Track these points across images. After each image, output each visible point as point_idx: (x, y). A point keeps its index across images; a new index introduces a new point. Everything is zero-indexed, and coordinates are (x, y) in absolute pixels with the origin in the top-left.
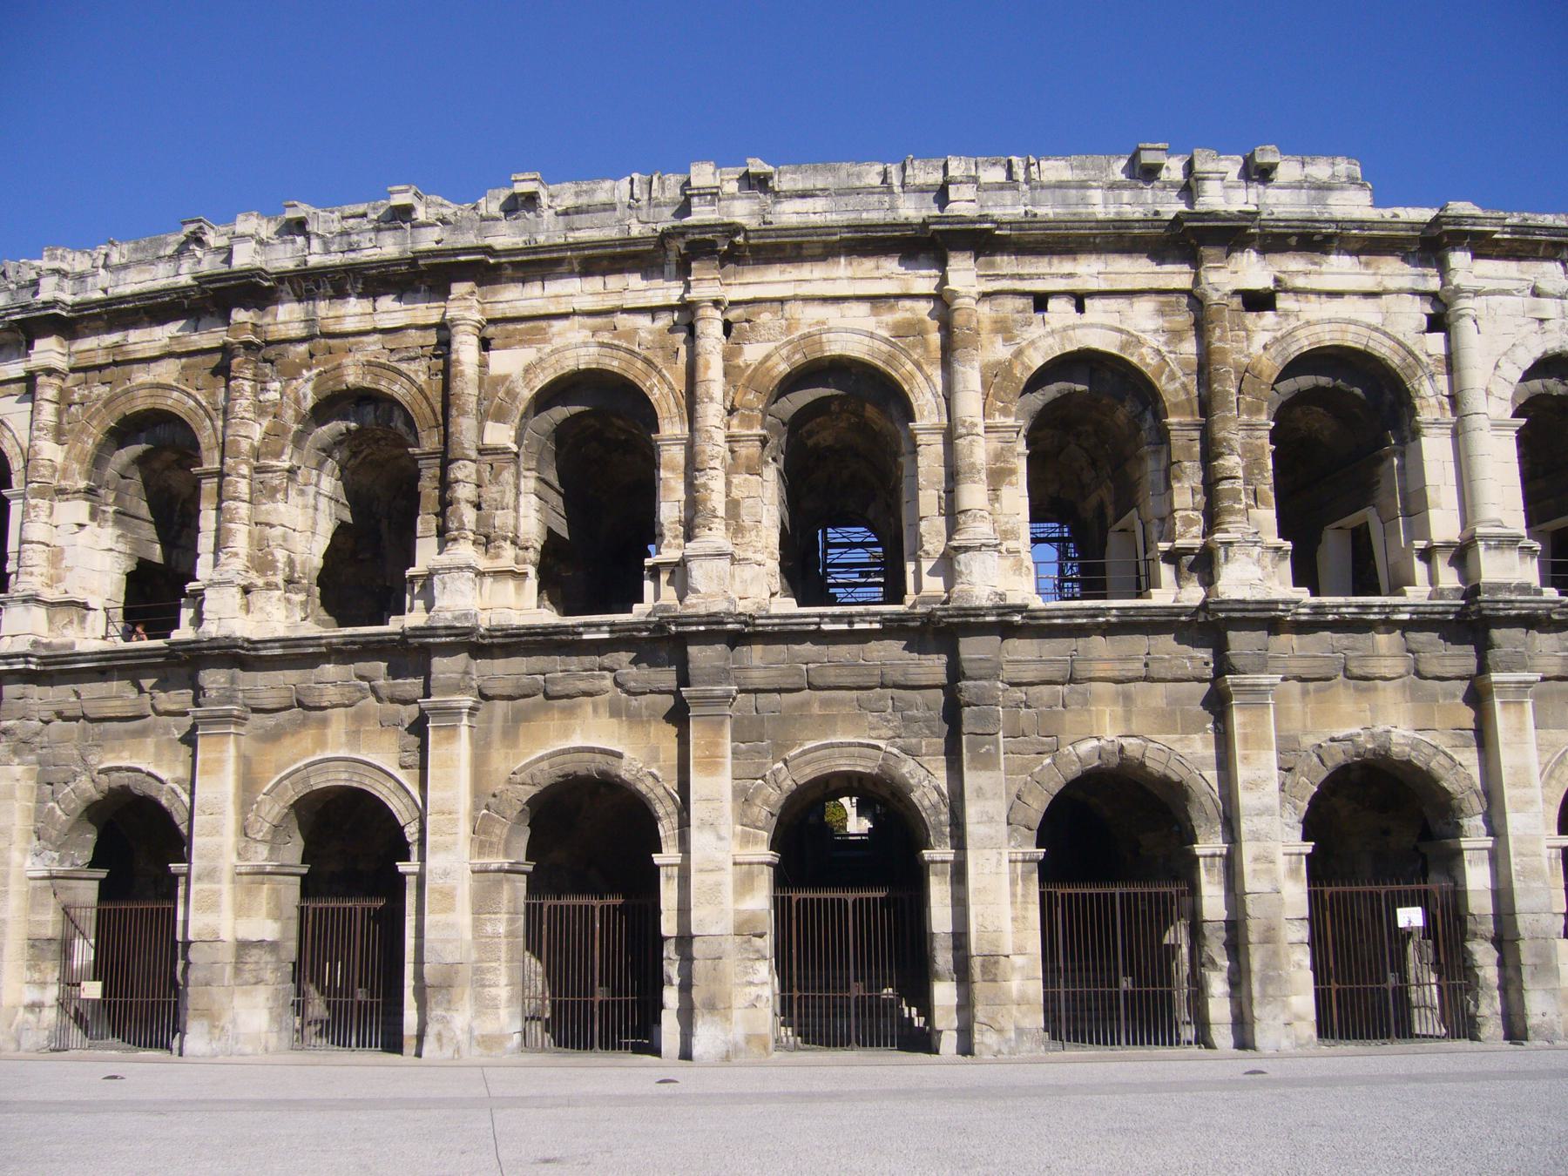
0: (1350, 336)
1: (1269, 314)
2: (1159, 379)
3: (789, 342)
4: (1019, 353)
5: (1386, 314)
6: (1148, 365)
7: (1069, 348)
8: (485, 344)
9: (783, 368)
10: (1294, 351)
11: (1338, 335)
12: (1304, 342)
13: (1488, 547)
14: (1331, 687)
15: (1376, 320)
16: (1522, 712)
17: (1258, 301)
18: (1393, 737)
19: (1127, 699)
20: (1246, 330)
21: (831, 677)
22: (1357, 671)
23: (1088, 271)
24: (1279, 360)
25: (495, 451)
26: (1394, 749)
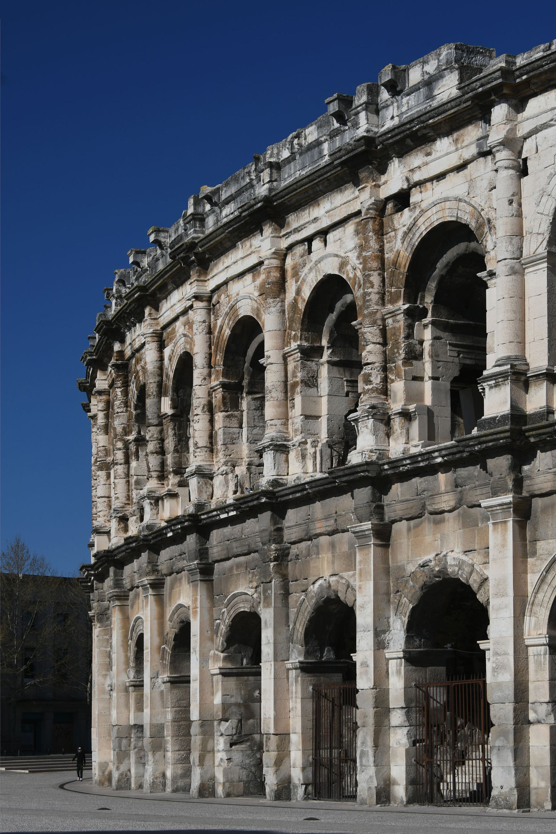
0: (447, 212)
2: (354, 289)
3: (227, 314)
6: (350, 279)
7: (320, 278)
9: (227, 332)
11: (440, 215)
13: (491, 387)
14: (421, 523)
16: (505, 530)
18: (450, 561)
19: (333, 546)
20: (395, 230)
21: (236, 548)
22: (430, 508)
24: (409, 250)
25: (165, 416)
26: (450, 570)
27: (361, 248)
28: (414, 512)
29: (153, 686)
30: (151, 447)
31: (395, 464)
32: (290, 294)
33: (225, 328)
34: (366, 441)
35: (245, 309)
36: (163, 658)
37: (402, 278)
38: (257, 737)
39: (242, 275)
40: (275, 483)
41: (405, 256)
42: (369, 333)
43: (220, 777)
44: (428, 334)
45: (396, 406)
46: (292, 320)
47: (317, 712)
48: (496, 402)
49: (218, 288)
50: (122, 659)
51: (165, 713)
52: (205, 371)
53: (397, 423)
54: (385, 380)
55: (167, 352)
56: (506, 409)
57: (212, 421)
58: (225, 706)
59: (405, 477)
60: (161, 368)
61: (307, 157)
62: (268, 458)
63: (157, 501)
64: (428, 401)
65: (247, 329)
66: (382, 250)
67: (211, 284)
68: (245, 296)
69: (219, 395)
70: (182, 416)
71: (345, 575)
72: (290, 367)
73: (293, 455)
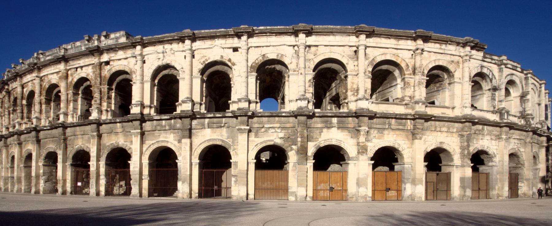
1: (109, 66)
4: (73, 79)
5: (129, 63)
9: (47, 86)
10: (112, 72)
12: (114, 70)
15: (126, 64)
17: (107, 63)
23: (82, 62)
27: (94, 72)
30: (18, 111)
32: (70, 79)
33: (46, 85)
35: (54, 81)
57: (41, 107)
63: (20, 124)
65: (54, 86)
66: (100, 74)
70: (30, 105)
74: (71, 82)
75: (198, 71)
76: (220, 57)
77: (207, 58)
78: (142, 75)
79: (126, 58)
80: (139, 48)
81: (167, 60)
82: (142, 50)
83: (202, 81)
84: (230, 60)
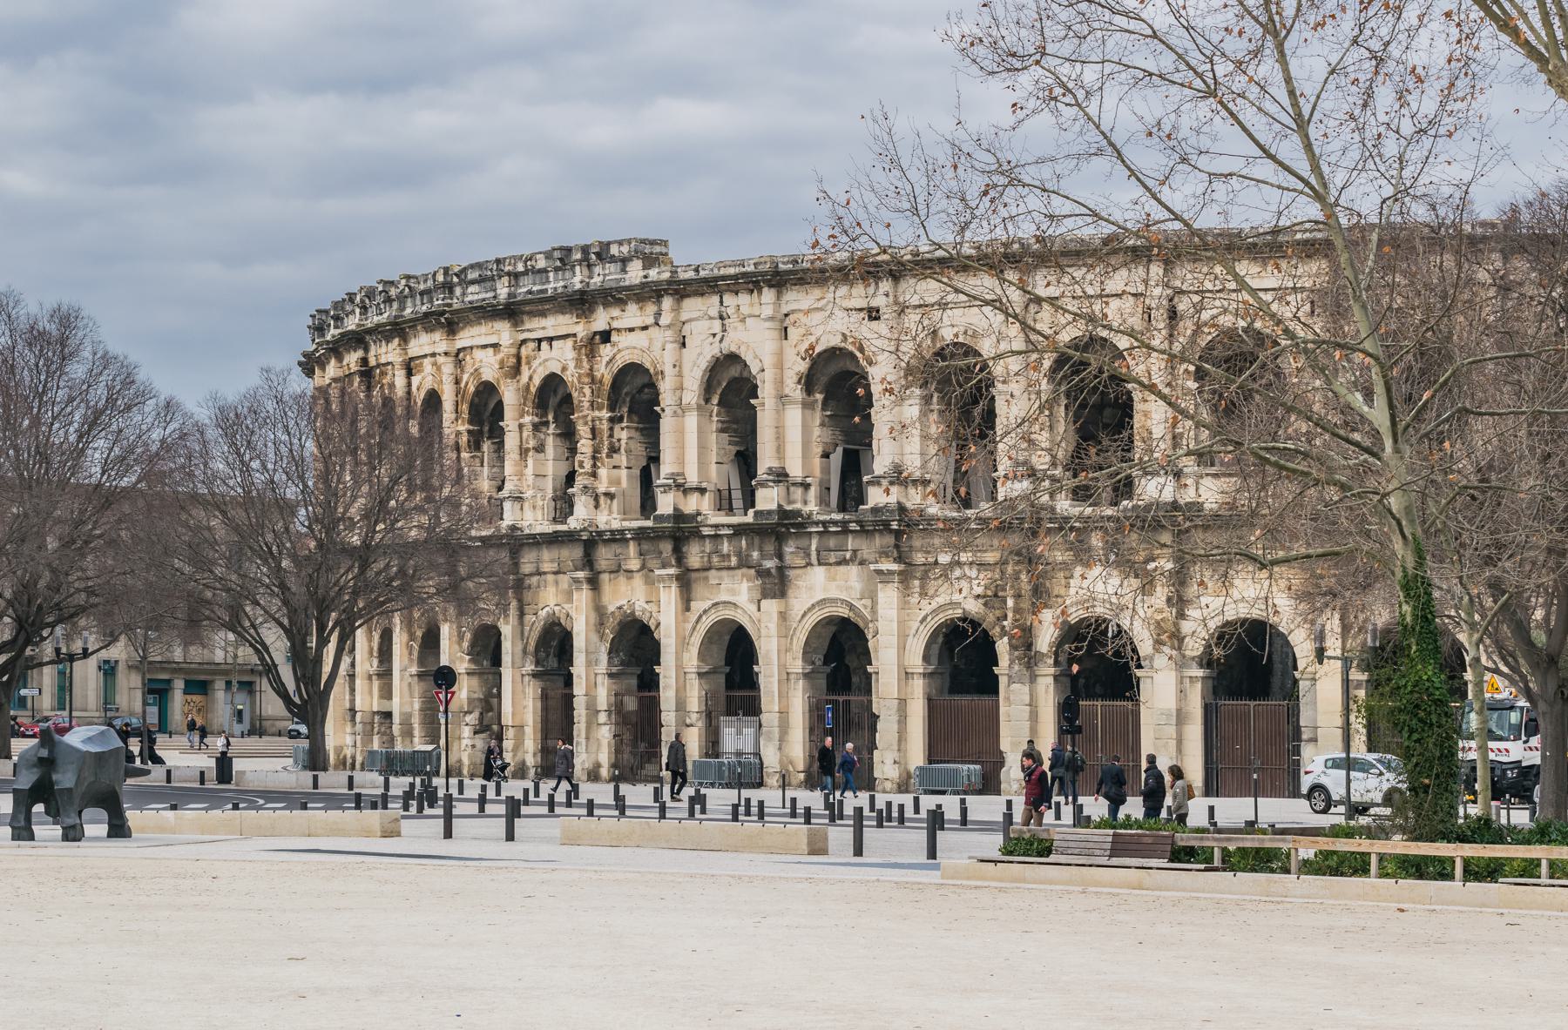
4: (531, 378)
8: (410, 373)
9: (472, 389)
17: (606, 336)
28: (614, 568)
29: (402, 679)
31: (600, 533)
32: (524, 378)
34: (582, 514)
35: (489, 375)
36: (410, 654)
37: (606, 393)
38: (495, 727)
39: (485, 347)
40: (513, 528)
41: (608, 379)
42: (583, 430)
43: (466, 761)
44: (624, 435)
45: (602, 489)
46: (525, 399)
47: (545, 709)
48: (666, 503)
49: (464, 349)
50: (366, 648)
51: (412, 704)
52: (454, 416)
53: (602, 499)
54: (594, 465)
55: (415, 380)
56: (670, 511)
58: (470, 701)
59: (606, 541)
60: (409, 393)
61: (538, 277)
62: (507, 505)
64: (624, 484)
65: (487, 390)
67: (459, 344)
68: (488, 366)
69: (465, 438)
71: (566, 606)
72: (525, 434)
73: (526, 505)
74: (528, 387)
75: (795, 379)
76: (839, 338)
77: (812, 339)
78: (680, 388)
79: (645, 328)
80: (667, 302)
81: (730, 345)
82: (676, 310)
83: (807, 406)
84: (861, 349)
